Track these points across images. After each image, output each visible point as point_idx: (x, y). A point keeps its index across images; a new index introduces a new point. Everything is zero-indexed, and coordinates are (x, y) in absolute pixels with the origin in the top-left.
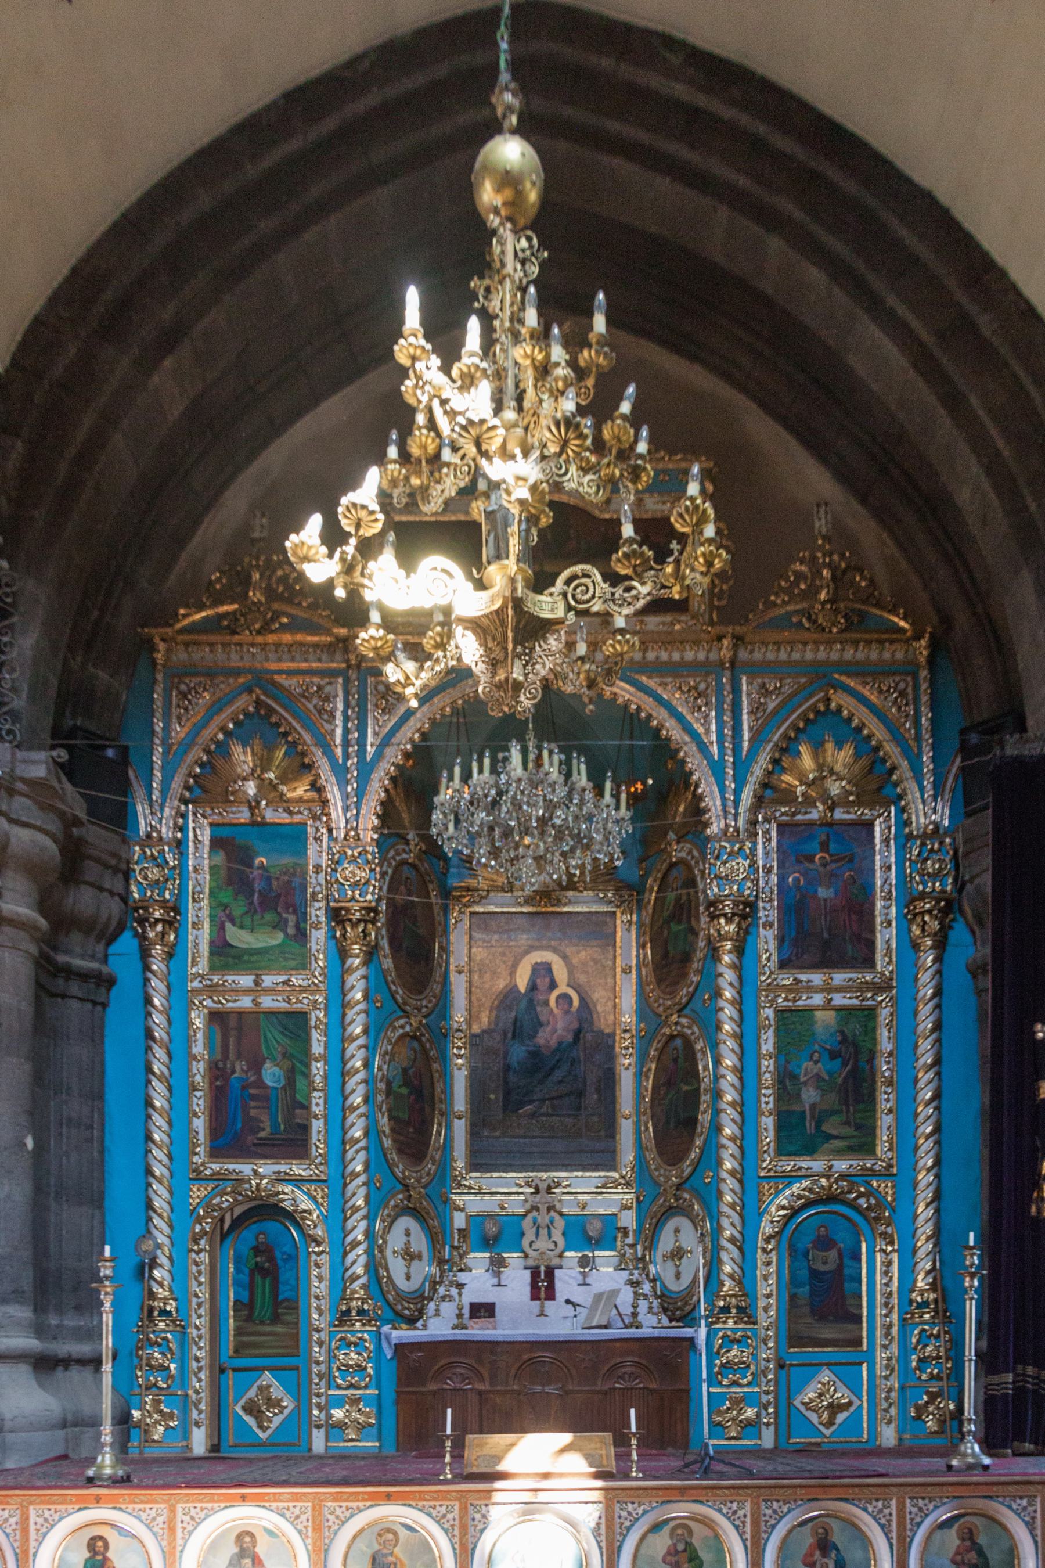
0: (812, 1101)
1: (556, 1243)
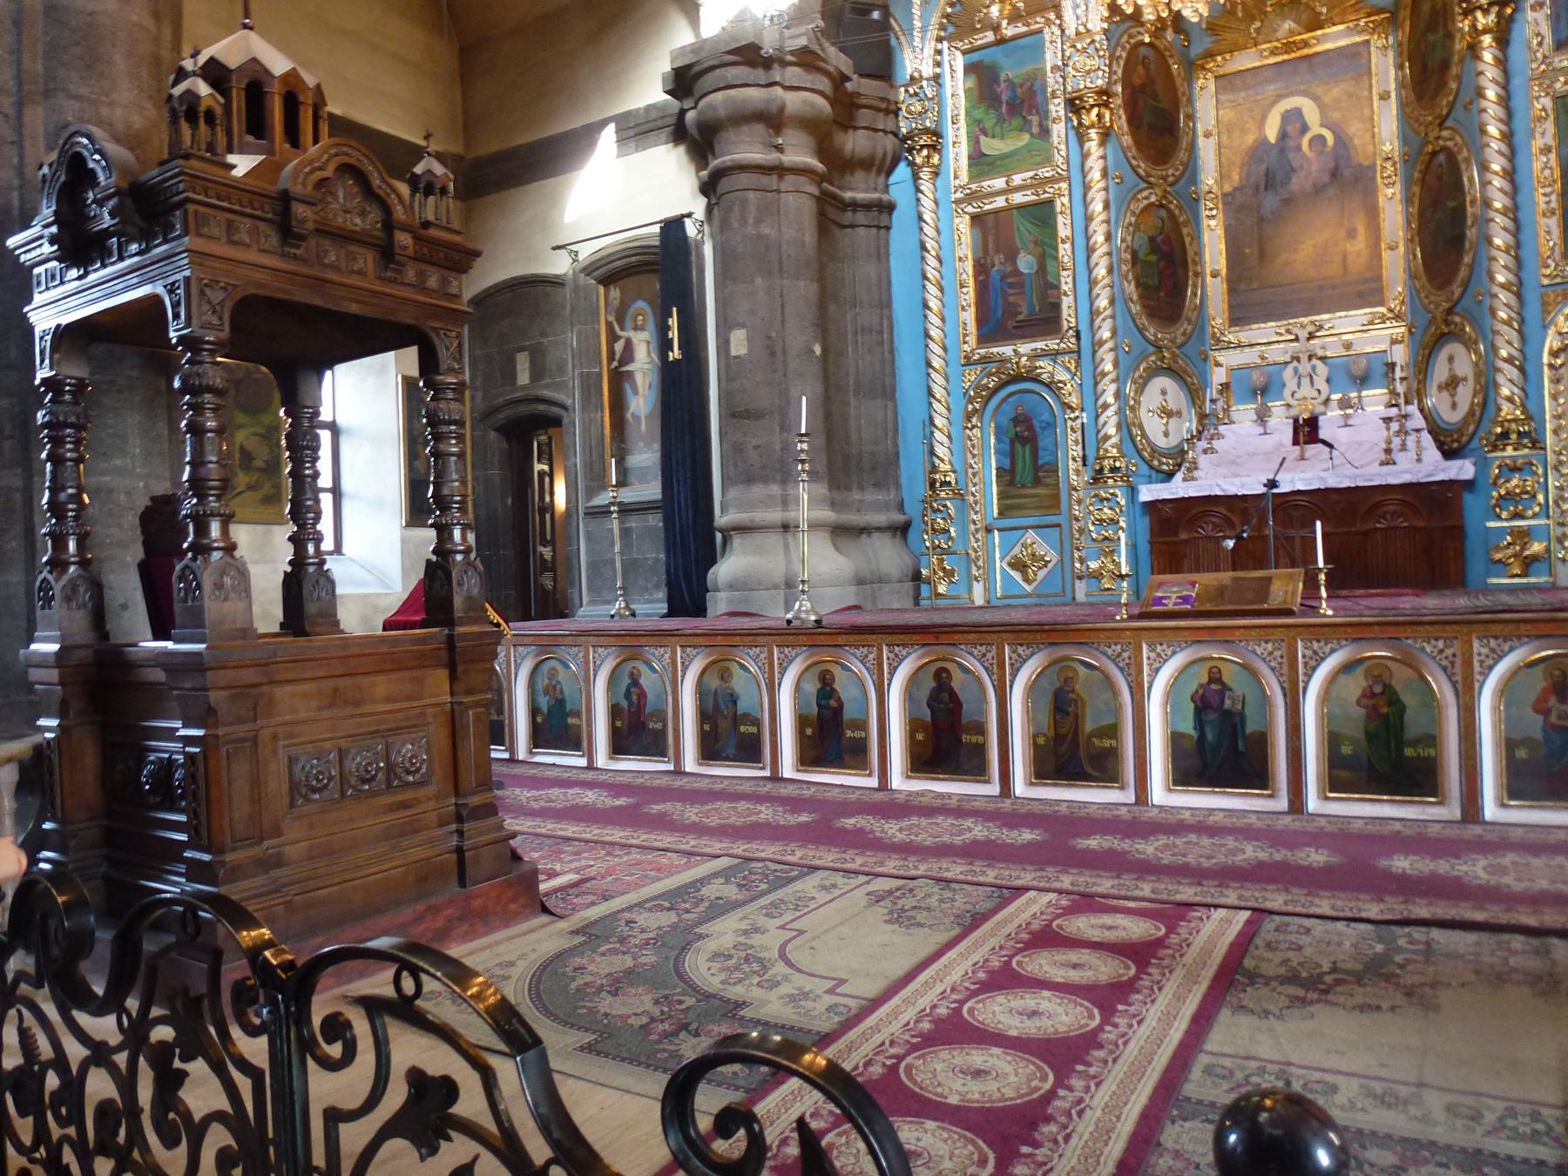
1: (1319, 391)
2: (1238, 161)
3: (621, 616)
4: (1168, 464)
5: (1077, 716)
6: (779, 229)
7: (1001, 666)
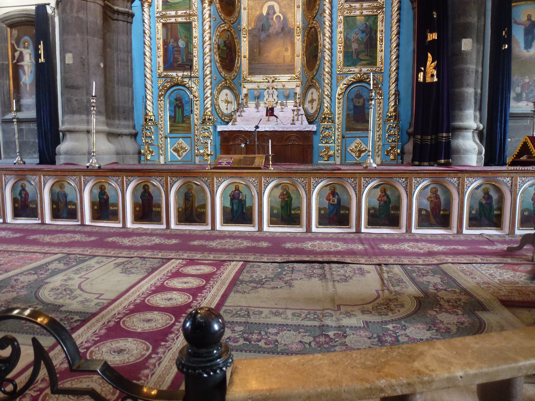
0: (355, 48)
2: (254, 20)
3: (19, 164)
4: (227, 119)
5: (192, 201)
6: (87, 16)
7: (167, 184)
